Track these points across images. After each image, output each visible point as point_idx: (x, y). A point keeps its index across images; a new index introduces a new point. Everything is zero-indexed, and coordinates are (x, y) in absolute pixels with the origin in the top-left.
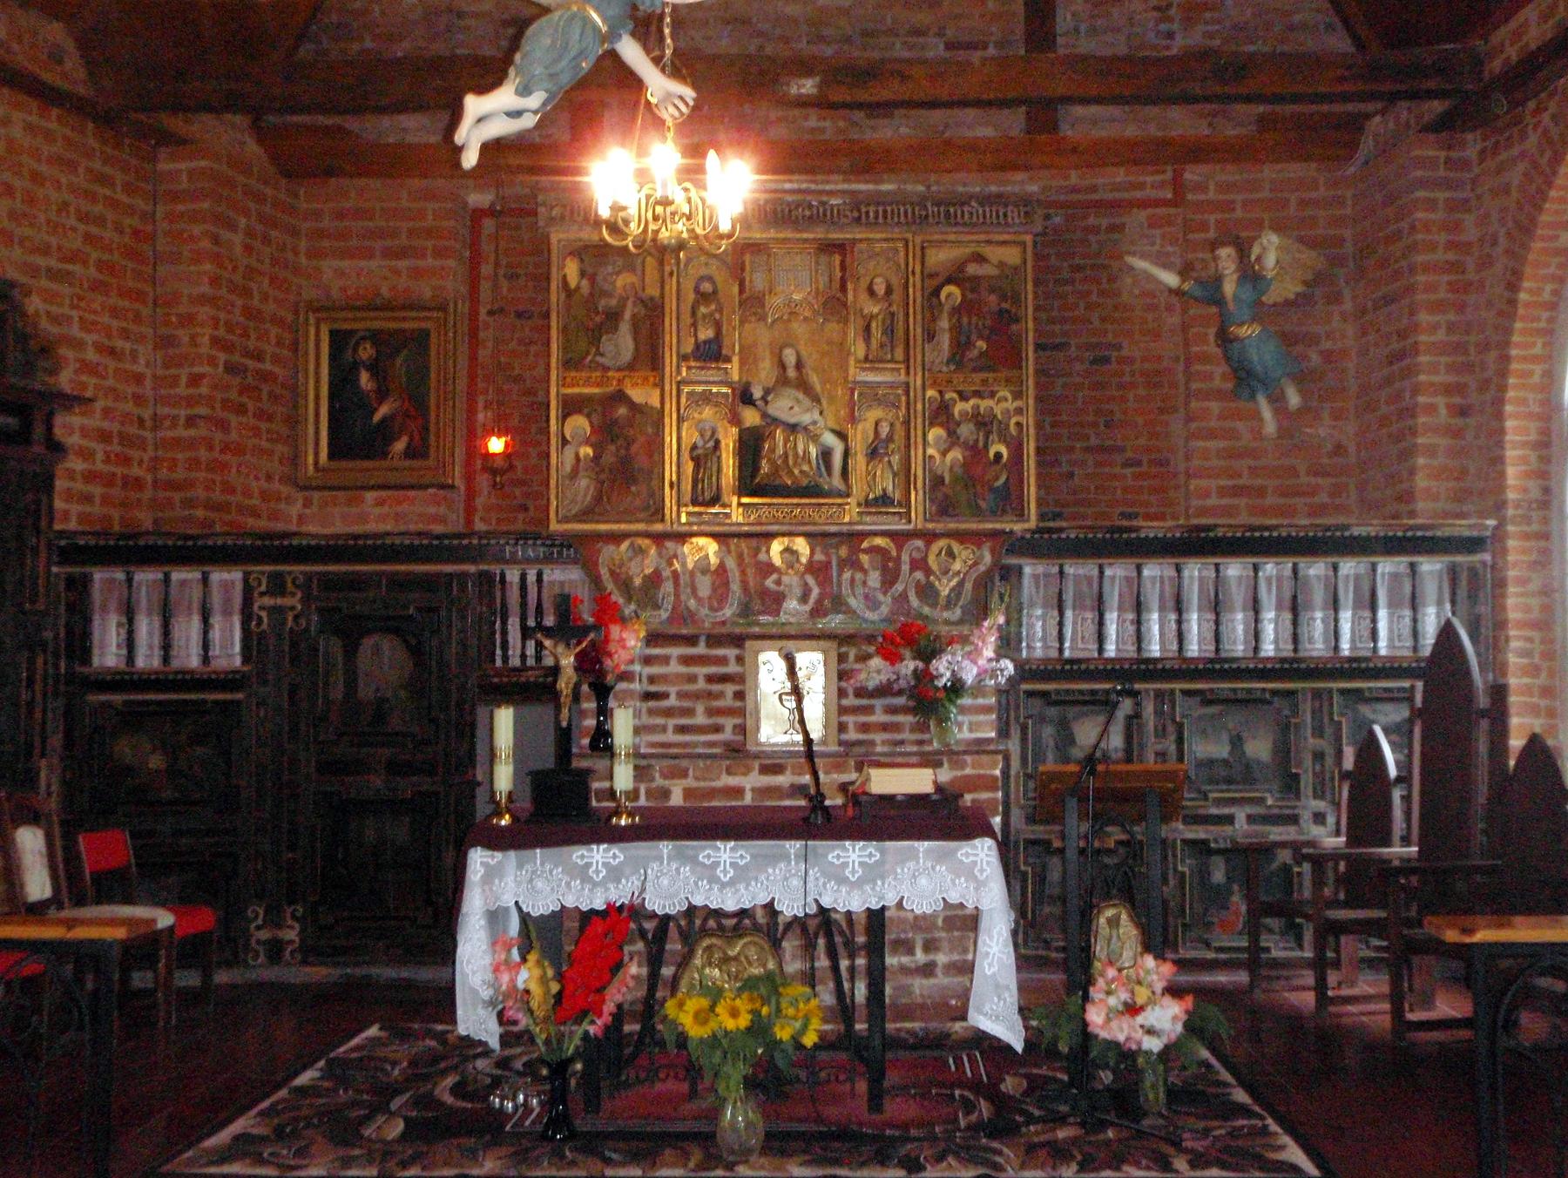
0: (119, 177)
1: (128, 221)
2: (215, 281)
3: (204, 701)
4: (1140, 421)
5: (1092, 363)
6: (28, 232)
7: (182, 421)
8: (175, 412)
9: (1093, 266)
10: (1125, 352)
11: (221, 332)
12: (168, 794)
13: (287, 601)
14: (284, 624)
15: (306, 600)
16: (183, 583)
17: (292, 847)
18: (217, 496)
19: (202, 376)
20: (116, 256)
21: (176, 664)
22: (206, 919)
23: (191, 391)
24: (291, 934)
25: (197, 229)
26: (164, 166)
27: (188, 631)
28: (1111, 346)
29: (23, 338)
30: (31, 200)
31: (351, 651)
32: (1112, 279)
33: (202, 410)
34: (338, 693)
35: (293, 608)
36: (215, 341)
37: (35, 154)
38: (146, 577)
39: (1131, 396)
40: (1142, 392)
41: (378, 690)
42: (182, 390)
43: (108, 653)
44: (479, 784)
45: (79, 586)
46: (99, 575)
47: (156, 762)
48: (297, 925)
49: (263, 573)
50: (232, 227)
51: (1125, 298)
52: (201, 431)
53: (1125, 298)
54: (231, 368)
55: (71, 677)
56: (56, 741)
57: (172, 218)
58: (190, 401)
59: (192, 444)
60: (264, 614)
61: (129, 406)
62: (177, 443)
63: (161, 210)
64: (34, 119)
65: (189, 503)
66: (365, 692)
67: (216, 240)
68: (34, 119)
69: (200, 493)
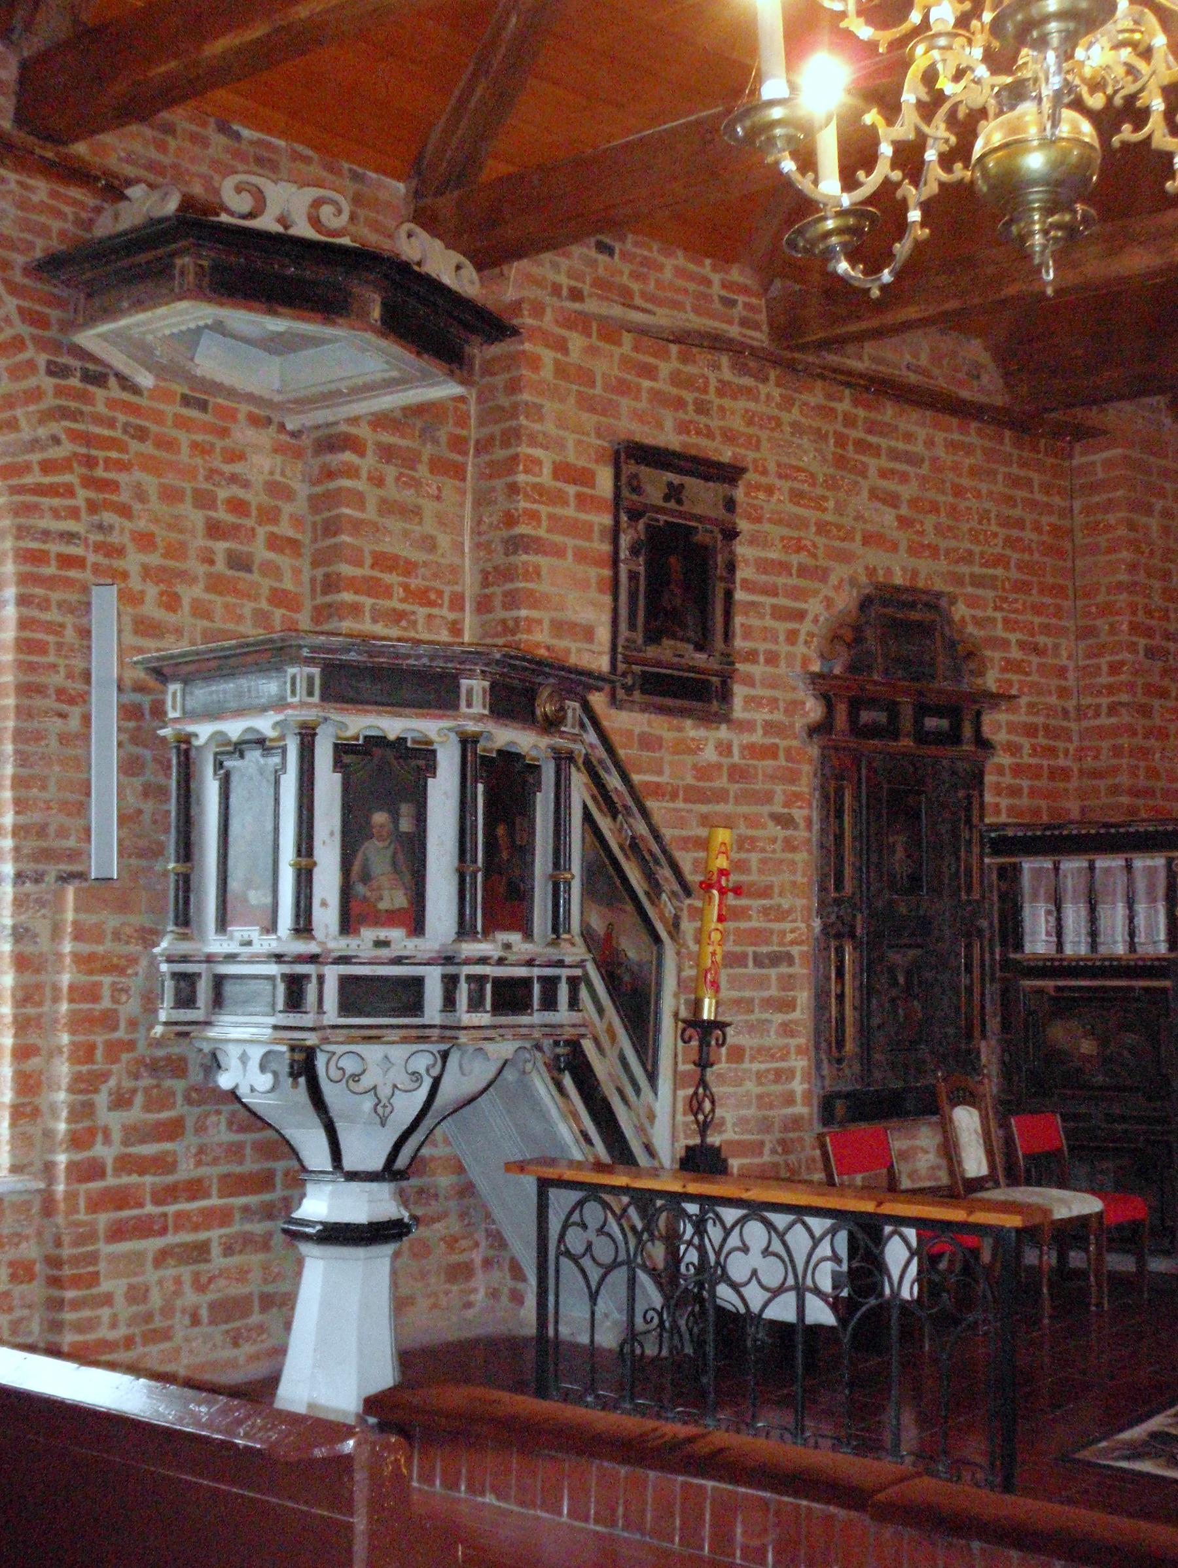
0: (1036, 477)
1: (1045, 520)
2: (1133, 567)
3: (1132, 988)
6: (953, 543)
7: (1104, 710)
8: (1098, 700)
11: (1141, 617)
12: (1100, 1079)
16: (1108, 871)
18: (1142, 782)
19: (1122, 663)
20: (1036, 556)
21: (1103, 950)
22: (1138, 1208)
23: (1111, 680)
25: (1111, 518)
26: (1077, 461)
27: (1114, 917)
29: (952, 645)
30: (953, 511)
33: (1125, 698)
36: (1134, 628)
37: (955, 468)
38: (1072, 865)
42: (1104, 679)
43: (1038, 941)
45: (1010, 875)
46: (1028, 865)
47: (1087, 1047)
50: (1149, 510)
52: (1125, 718)
54: (1150, 653)
55: (1006, 964)
56: (994, 1024)
57: (1088, 510)
58: (1111, 689)
59: (1115, 731)
61: (1053, 700)
62: (1101, 732)
63: (1077, 505)
64: (956, 436)
65: (1114, 790)
67: (1132, 526)
68: (956, 436)
69: (1124, 780)
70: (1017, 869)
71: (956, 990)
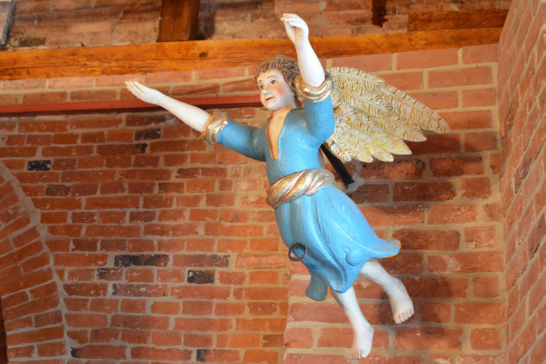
4: (242, 352)
5: (191, 280)
9: (206, 172)
10: (232, 268)
28: (214, 260)
32: (224, 185)
39: (233, 319)
40: (247, 315)
51: (238, 206)
53: (238, 206)
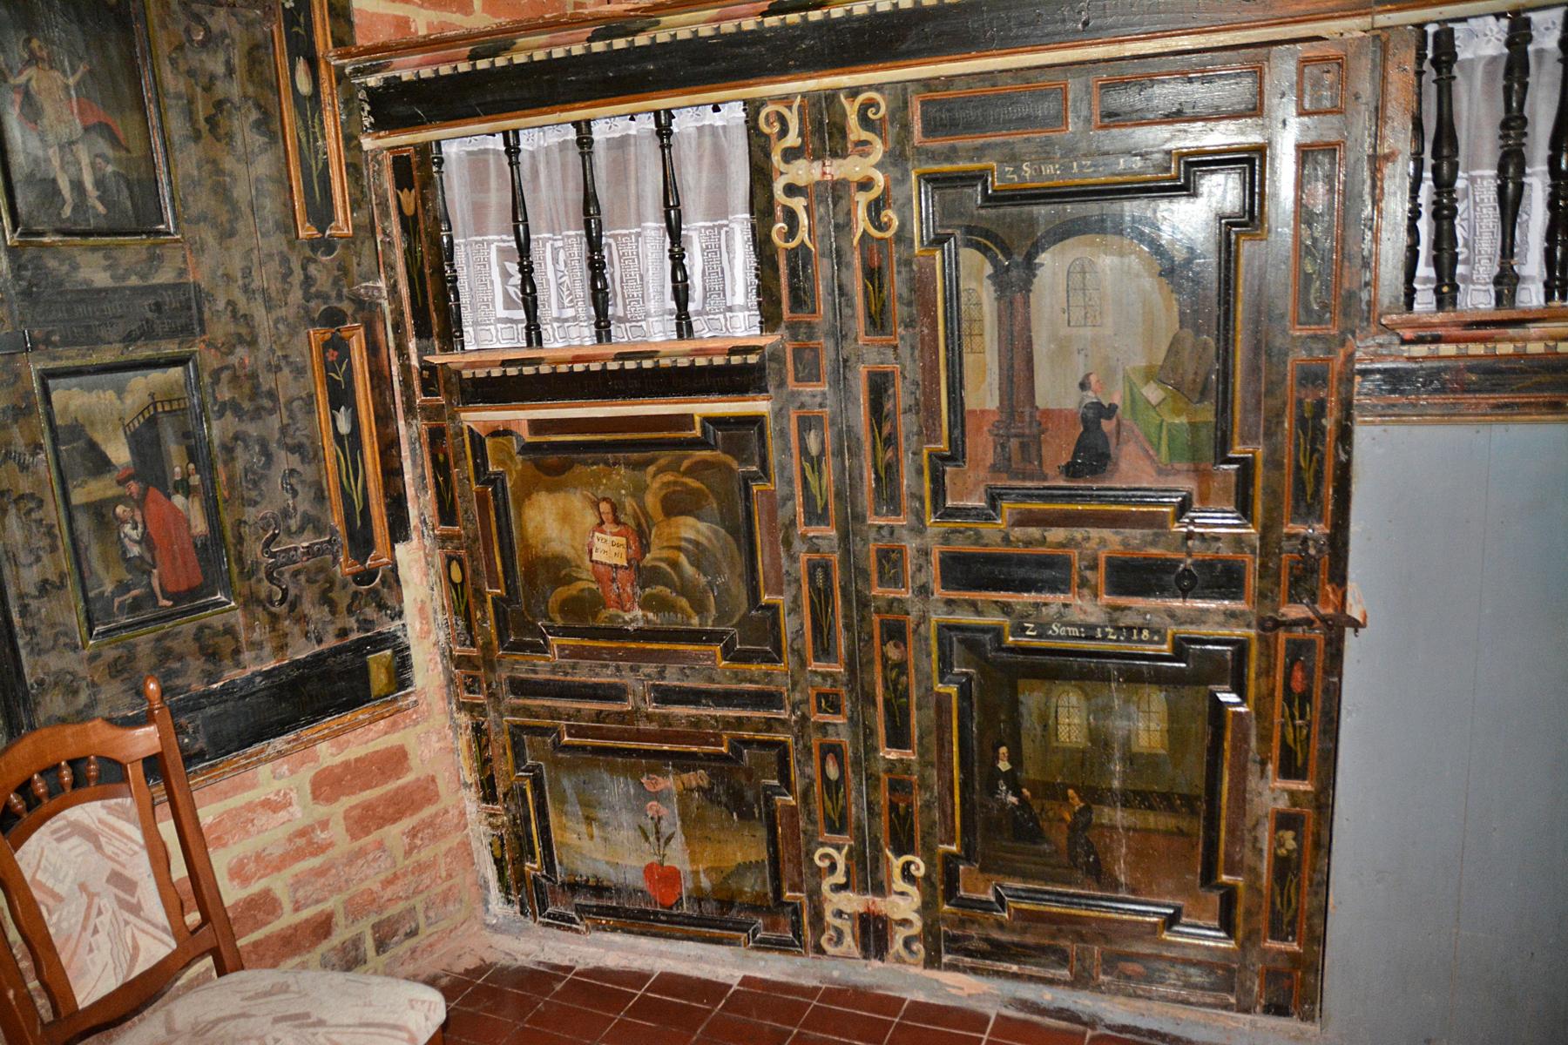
3: (685, 421)
12: (635, 616)
13: (851, 168)
14: (844, 227)
15: (896, 158)
16: (622, 143)
17: (898, 738)
21: (622, 336)
24: (903, 905)
27: (639, 253)
31: (1014, 283)
34: (983, 394)
35: (865, 185)
38: (545, 136)
41: (1084, 386)
44: (1357, 625)
45: (416, 172)
46: (462, 147)
47: (609, 549)
48: (913, 890)
49: (786, 99)
55: (432, 378)
56: (420, 506)
60: (798, 204)
66: (1055, 390)
70: (429, 157)
71: (307, 451)
